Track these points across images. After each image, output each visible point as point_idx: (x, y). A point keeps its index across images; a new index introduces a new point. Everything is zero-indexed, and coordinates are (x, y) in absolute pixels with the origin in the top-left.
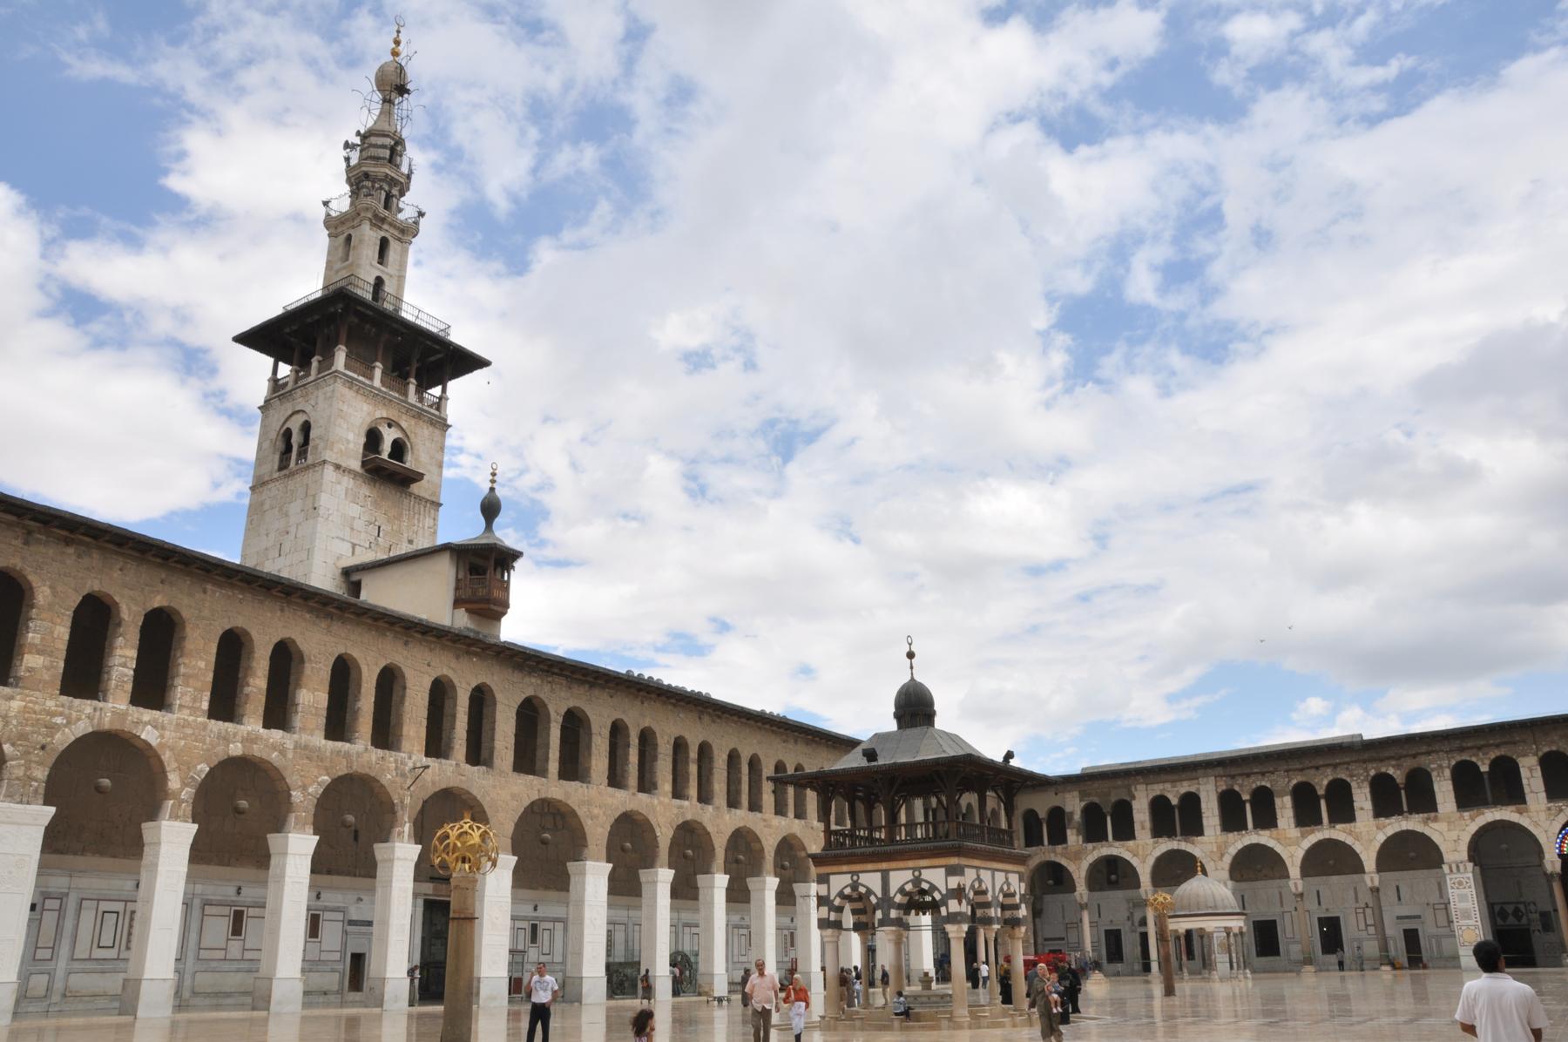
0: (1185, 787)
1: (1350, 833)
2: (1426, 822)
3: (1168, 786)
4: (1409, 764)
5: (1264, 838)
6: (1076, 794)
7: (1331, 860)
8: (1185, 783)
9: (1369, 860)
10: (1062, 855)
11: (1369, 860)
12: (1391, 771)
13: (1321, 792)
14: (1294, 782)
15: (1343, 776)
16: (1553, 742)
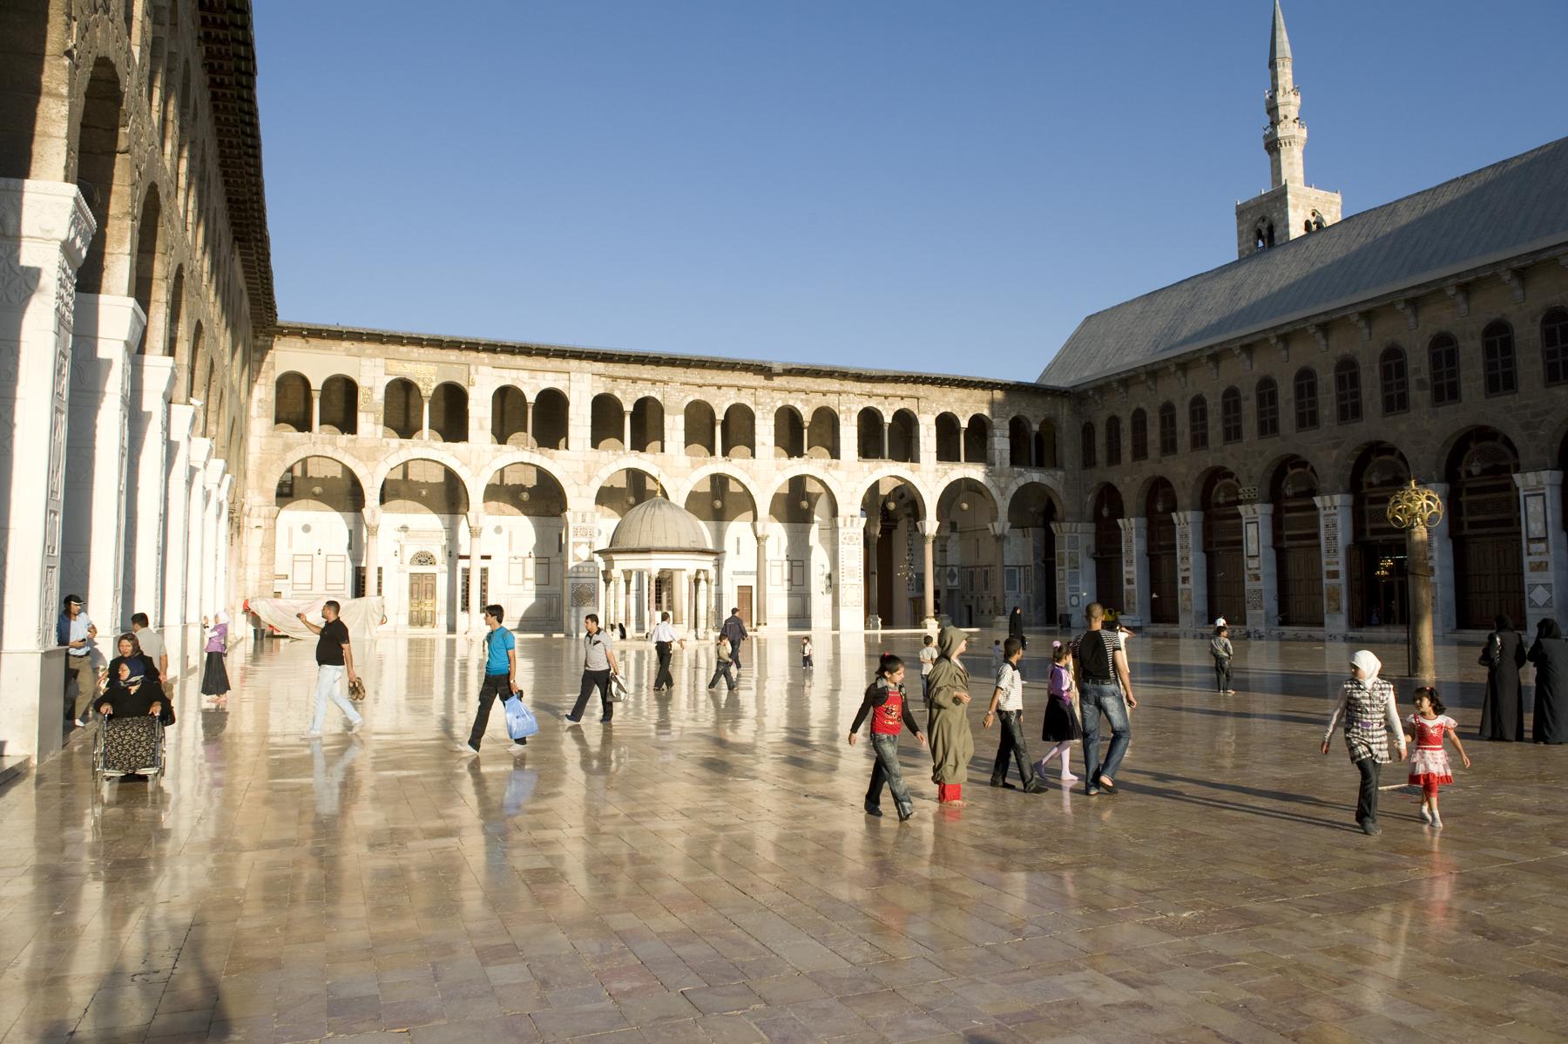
0: (549, 381)
1: (747, 470)
2: (826, 470)
3: (524, 375)
4: (818, 401)
5: (643, 461)
6: (380, 361)
7: (720, 501)
8: (549, 376)
9: (763, 503)
10: (346, 450)
11: (763, 503)
12: (799, 406)
13: (720, 416)
14: (691, 399)
15: (749, 404)
16: (949, 404)
